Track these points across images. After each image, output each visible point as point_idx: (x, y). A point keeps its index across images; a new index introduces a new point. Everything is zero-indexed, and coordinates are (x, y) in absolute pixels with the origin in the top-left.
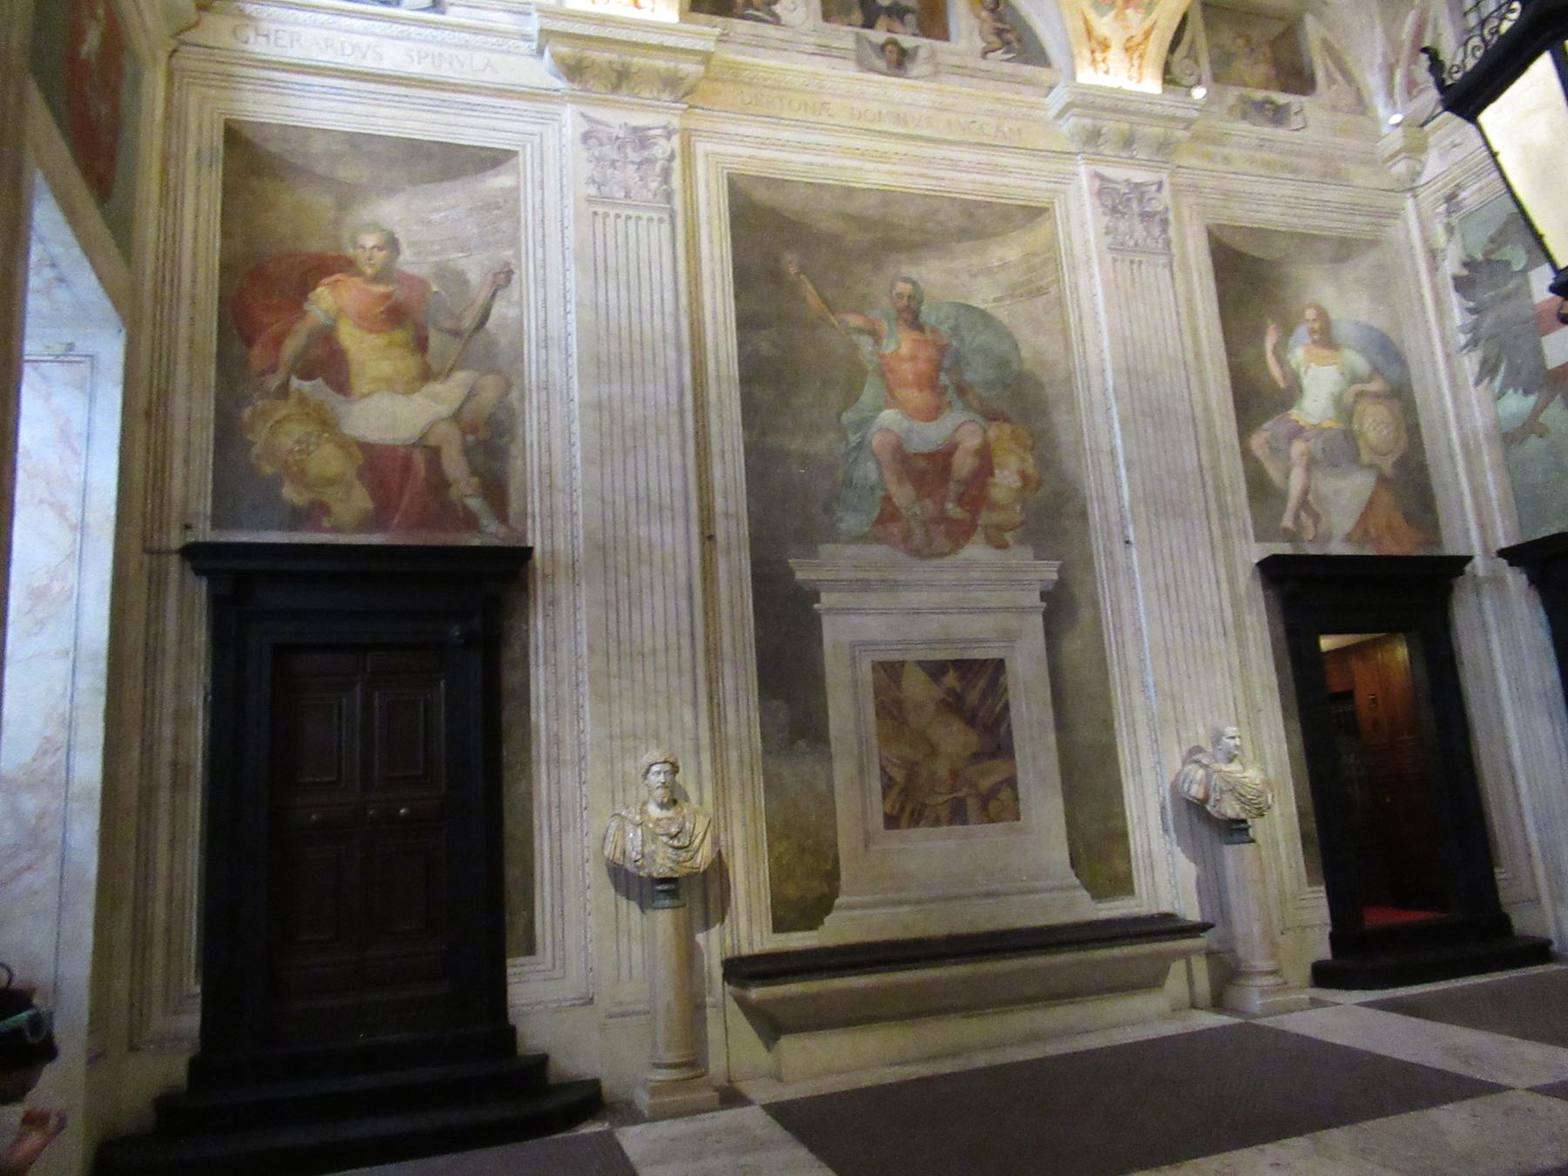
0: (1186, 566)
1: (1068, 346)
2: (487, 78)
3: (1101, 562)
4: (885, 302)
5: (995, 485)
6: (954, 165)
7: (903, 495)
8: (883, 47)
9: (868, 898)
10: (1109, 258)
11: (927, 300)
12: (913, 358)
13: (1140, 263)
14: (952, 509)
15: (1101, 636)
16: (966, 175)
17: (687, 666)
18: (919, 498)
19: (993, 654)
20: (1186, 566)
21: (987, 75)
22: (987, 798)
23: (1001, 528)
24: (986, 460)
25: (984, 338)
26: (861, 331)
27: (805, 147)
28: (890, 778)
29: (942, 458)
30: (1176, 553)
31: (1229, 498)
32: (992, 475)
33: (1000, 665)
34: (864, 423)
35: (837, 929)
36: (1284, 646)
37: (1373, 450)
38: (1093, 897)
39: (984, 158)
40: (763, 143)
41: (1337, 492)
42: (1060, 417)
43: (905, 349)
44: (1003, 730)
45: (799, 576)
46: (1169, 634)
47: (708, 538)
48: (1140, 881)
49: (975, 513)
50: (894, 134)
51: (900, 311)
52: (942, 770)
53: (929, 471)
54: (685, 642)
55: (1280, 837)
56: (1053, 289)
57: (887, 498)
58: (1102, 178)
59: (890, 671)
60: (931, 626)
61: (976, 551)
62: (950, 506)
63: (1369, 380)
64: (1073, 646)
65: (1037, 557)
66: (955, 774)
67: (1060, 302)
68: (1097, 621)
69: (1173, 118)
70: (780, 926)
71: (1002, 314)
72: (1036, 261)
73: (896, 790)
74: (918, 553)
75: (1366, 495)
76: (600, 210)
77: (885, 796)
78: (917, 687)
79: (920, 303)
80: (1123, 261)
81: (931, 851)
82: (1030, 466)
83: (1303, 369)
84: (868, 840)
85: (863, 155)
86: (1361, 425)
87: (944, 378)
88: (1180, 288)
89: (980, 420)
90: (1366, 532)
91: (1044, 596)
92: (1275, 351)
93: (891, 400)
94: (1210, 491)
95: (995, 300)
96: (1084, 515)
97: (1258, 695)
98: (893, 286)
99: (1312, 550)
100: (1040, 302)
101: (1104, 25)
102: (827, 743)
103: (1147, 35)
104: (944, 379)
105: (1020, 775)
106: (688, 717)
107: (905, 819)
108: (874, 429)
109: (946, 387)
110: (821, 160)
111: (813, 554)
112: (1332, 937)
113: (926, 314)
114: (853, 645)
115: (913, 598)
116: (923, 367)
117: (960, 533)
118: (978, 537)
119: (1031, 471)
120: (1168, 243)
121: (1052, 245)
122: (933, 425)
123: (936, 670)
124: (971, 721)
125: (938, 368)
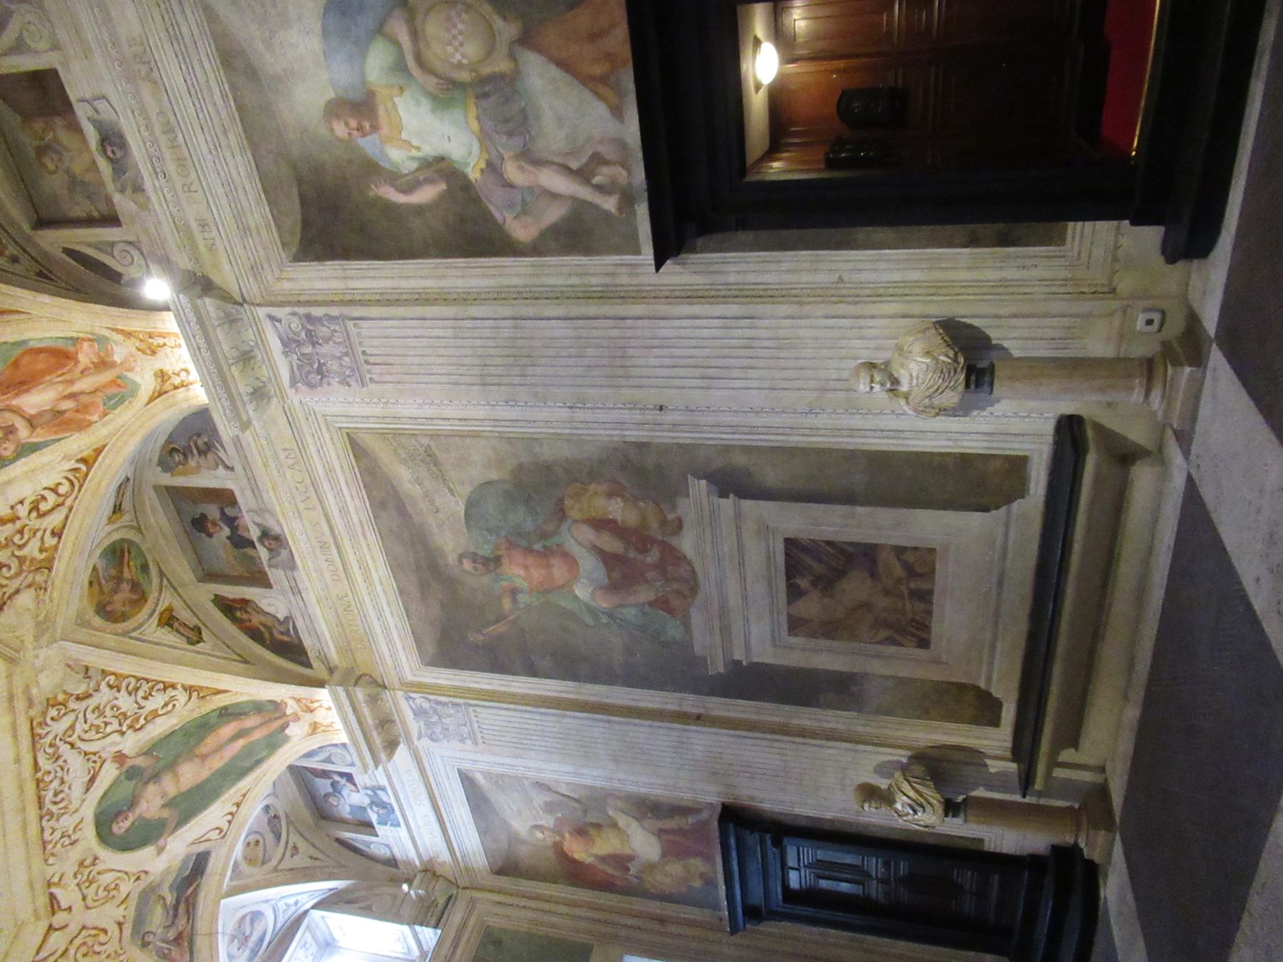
0: (677, 352)
1: (475, 435)
2: (415, 773)
3: (685, 437)
4: (486, 580)
5: (623, 521)
6: (344, 510)
7: (645, 595)
8: (270, 550)
9: (984, 668)
10: (371, 386)
11: (472, 549)
12: (526, 568)
13: (364, 353)
14: (653, 557)
15: (759, 448)
16: (348, 503)
17: (794, 746)
18: (647, 581)
19: (780, 547)
20: (677, 352)
21: (247, 466)
22: (911, 572)
23: (664, 522)
24: (601, 524)
25: (490, 507)
26: (514, 600)
27: (380, 616)
28: (887, 639)
29: (609, 560)
30: (667, 362)
31: (594, 280)
32: (614, 521)
33: (791, 543)
34: (592, 611)
35: (1005, 688)
36: (763, 235)
37: (490, 52)
38: (1023, 497)
39: (326, 486)
40: (390, 642)
41: (560, 121)
42: (547, 453)
43: (521, 572)
44: (851, 549)
45: (722, 670)
46: (755, 384)
47: (698, 719)
48: (1015, 448)
49: (654, 541)
50: (338, 548)
51: (490, 571)
52: (882, 602)
53: (620, 574)
54: (776, 744)
55: (994, 275)
56: (425, 441)
57: (651, 604)
58: (293, 382)
59: (796, 625)
60: (758, 589)
61: (687, 544)
62: (649, 560)
63: (397, 43)
64: (771, 476)
65: (687, 496)
66: (887, 593)
67: (435, 436)
68: (747, 450)
69: (200, 321)
70: (995, 722)
71: (466, 490)
72: (399, 451)
73: (898, 638)
74: (694, 589)
75: (554, 71)
76: (480, 741)
77: (901, 645)
78: (811, 606)
79: (475, 554)
80: (369, 371)
81: (953, 619)
82: (603, 488)
83: (414, 153)
84: (937, 661)
85: (368, 578)
86: (460, 66)
87: (541, 546)
88: (374, 311)
89: (569, 521)
90: (603, 79)
91: (723, 495)
92: (406, 191)
93: (566, 588)
94: (593, 310)
95: (453, 494)
96: (642, 446)
97: (823, 278)
98: (466, 572)
99: (639, 176)
100: (441, 455)
101: (145, 382)
102: (854, 675)
103: (128, 334)
104: (537, 547)
105: (893, 542)
106: (832, 751)
107: (924, 635)
108: (594, 604)
109: (544, 547)
110: (385, 607)
111: (704, 659)
112: (1134, 223)
113: (486, 550)
114: (775, 646)
115: (734, 599)
116: (530, 560)
117: (672, 556)
118: (674, 541)
119: (603, 488)
120: (332, 319)
121: (383, 435)
122: (581, 562)
123: (794, 593)
124: (841, 573)
125: (529, 550)
